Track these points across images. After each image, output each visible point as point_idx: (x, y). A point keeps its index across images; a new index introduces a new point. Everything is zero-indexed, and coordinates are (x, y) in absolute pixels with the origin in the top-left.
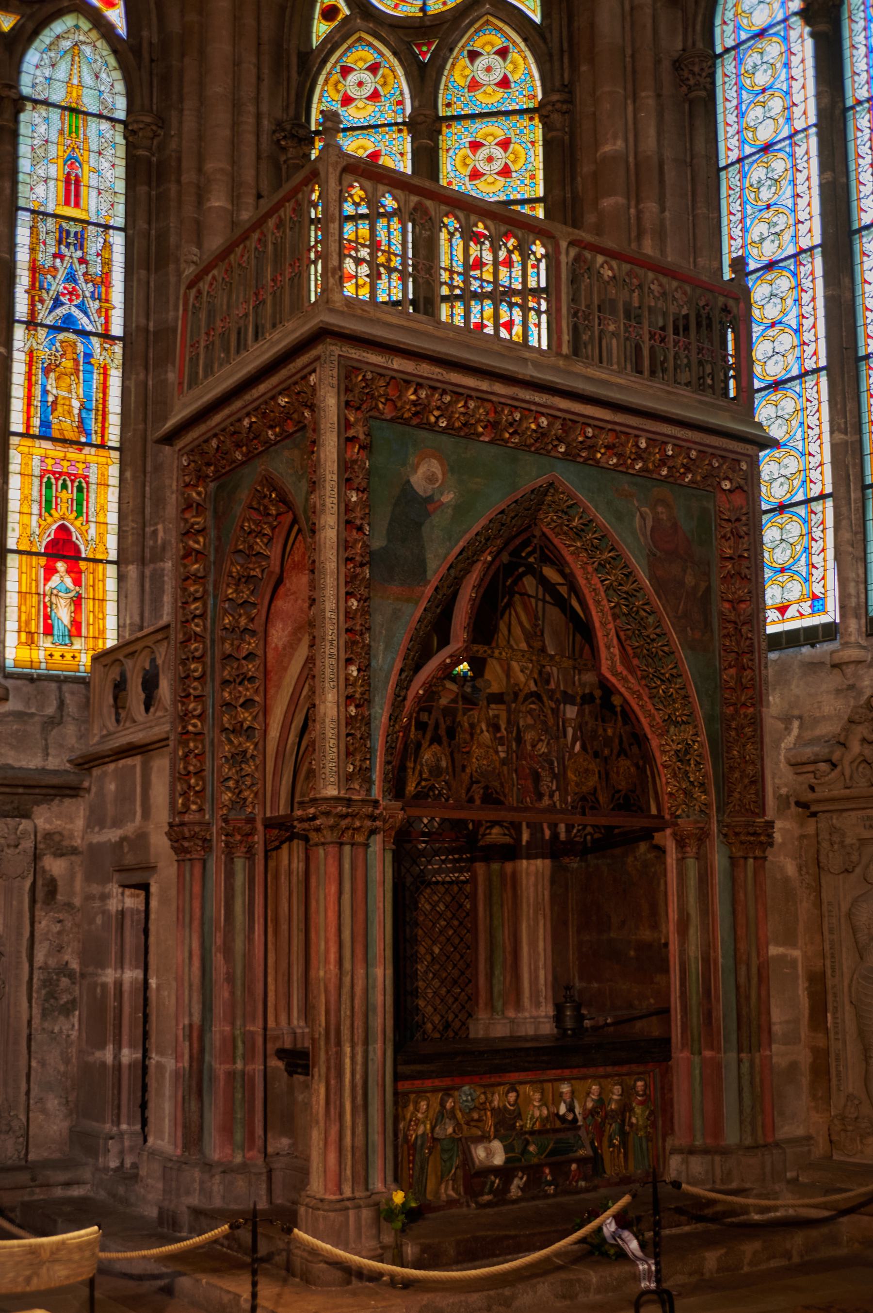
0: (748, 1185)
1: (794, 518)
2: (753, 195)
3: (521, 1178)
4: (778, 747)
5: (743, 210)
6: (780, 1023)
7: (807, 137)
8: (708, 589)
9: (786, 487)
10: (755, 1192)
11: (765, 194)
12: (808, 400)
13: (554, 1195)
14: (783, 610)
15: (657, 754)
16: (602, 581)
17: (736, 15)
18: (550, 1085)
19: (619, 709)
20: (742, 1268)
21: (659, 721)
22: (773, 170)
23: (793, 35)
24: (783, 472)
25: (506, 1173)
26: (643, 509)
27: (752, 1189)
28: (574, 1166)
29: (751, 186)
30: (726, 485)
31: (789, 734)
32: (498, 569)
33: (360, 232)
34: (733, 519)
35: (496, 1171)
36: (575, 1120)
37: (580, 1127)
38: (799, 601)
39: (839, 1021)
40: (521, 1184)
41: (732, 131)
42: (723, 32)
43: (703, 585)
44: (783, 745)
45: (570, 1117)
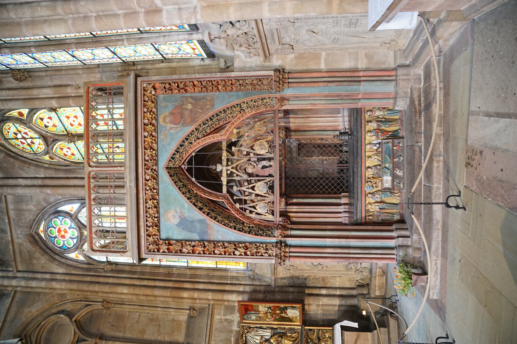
0: (410, 86)
3: (397, 171)
6: (350, 62)
8: (192, 97)
10: (413, 85)
13: (404, 157)
15: (252, 113)
16: (195, 141)
18: (366, 153)
19: (238, 130)
20: (441, 114)
21: (240, 115)
25: (394, 177)
26: (168, 129)
27: (412, 85)
28: (395, 148)
30: (153, 92)
32: (198, 182)
33: (108, 213)
34: (165, 90)
35: (393, 181)
36: (379, 143)
37: (382, 142)
40: (398, 171)
43: (190, 100)
44: (245, 59)
45: (378, 145)
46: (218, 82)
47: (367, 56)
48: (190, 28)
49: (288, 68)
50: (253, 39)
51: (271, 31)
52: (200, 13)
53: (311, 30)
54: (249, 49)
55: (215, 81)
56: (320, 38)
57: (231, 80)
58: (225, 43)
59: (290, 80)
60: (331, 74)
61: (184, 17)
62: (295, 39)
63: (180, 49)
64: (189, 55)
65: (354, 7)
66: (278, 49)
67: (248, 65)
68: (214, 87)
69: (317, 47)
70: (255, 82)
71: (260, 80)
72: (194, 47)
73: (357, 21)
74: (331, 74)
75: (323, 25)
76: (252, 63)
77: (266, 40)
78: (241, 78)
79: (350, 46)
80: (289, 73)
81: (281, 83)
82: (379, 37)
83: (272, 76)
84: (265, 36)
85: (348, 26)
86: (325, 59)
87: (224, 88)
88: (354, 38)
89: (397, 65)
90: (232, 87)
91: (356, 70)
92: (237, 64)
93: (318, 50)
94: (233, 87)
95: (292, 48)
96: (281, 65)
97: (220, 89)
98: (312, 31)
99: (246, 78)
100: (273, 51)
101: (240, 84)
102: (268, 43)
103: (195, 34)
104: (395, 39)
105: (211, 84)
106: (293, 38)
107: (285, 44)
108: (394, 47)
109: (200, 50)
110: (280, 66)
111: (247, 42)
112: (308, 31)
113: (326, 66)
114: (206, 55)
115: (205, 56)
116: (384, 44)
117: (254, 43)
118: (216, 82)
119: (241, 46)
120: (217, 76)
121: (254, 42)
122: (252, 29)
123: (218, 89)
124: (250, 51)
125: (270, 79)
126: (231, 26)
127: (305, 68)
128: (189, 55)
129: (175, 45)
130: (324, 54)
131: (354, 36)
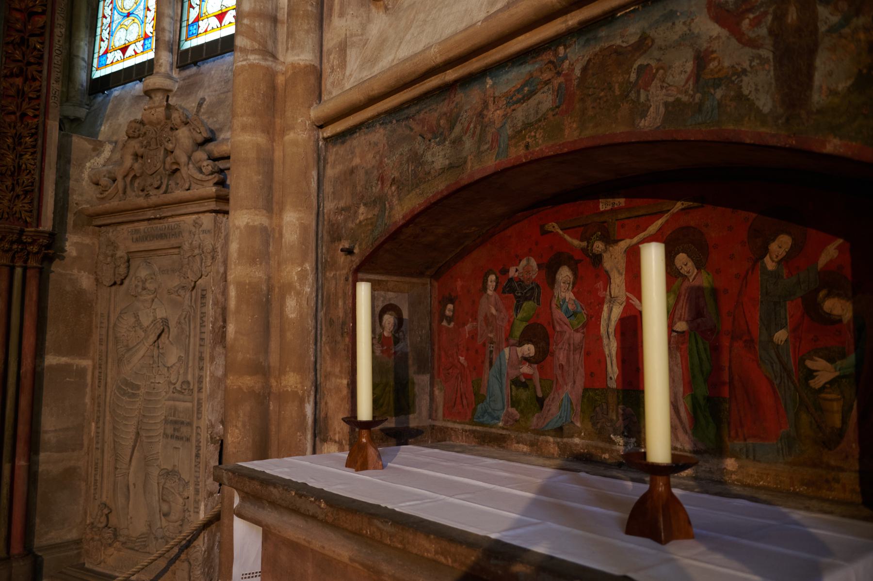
4: (81, 165)
31: (98, 155)
39: (100, 430)
44: (88, 165)
46: (34, 79)
47: (70, 473)
48: (187, 50)
49: (56, 268)
50: (158, 188)
51: (176, 233)
52: (263, 63)
53: (166, 330)
54: (125, 176)
55: (41, 72)
56: (141, 353)
57: (35, 116)
58: (154, 118)
59: (19, 271)
60: (27, 382)
61: (257, 24)
62: (144, 289)
63: (129, 15)
64: (105, 35)
65: (244, 426)
66: (116, 248)
67: (73, 171)
68: (20, 64)
69: (110, 345)
70: (25, 178)
71: (26, 193)
72: (130, 52)
73: (182, 439)
74: (27, 382)
75: (180, 358)
76: (77, 180)
77: (149, 220)
78: (40, 142)
79: (108, 427)
80: (41, 271)
81: (15, 246)
82: (128, 498)
83: (38, 224)
84: (160, 218)
85: (171, 418)
86: (71, 365)
87: (12, 92)
88: (132, 436)
89: (40, 554)
90: (14, 113)
91: (34, 445)
92: (79, 143)
93: (103, 348)
94: (13, 117)
95: (115, 284)
96: (64, 254)
97: (11, 80)
98: (163, 331)
99: (39, 156)
100: (110, 234)
101: (21, 137)
102: (136, 224)
103: (170, 60)
104: (122, 539)
105: (32, 60)
106: (147, 285)
107: (129, 267)
108: (97, 538)
109: (115, 64)
110: (63, 250)
111: (150, 172)
112: (165, 321)
113: (51, 367)
114: (101, 78)
115: (97, 74)
116: (106, 511)
117: (143, 190)
118: (35, 73)
119: (136, 156)
120: (52, 81)
121: (149, 188)
122: (187, 186)
123: (12, 75)
124: (120, 179)
125: (28, 219)
126: (200, 138)
127: (51, 313)
128: (105, 35)
129: (142, 7)
130: (86, 363)
131: (138, 434)
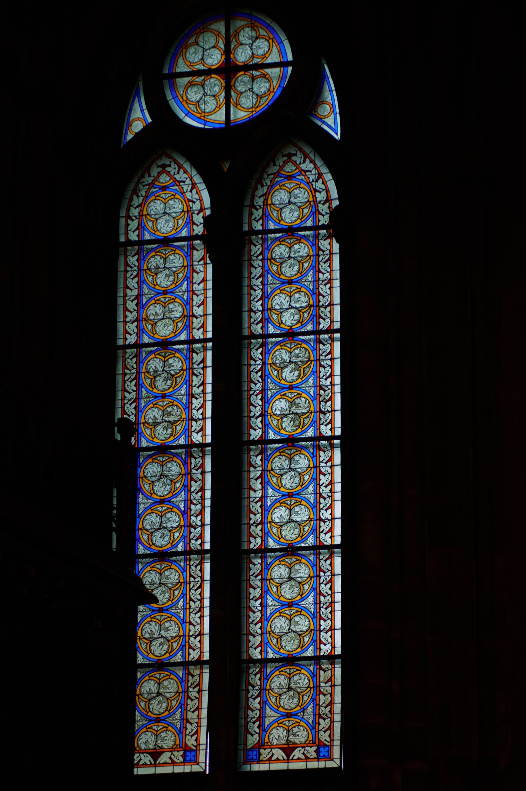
1: (172, 676)
2: (149, 381)
5: (138, 392)
7: (205, 349)
9: (165, 647)
11: (161, 385)
12: (191, 576)
14: (156, 754)
17: (141, 214)
22: (170, 366)
23: (197, 255)
24: (163, 633)
29: (148, 372)
38: (172, 750)
41: (130, 317)
42: (127, 225)
